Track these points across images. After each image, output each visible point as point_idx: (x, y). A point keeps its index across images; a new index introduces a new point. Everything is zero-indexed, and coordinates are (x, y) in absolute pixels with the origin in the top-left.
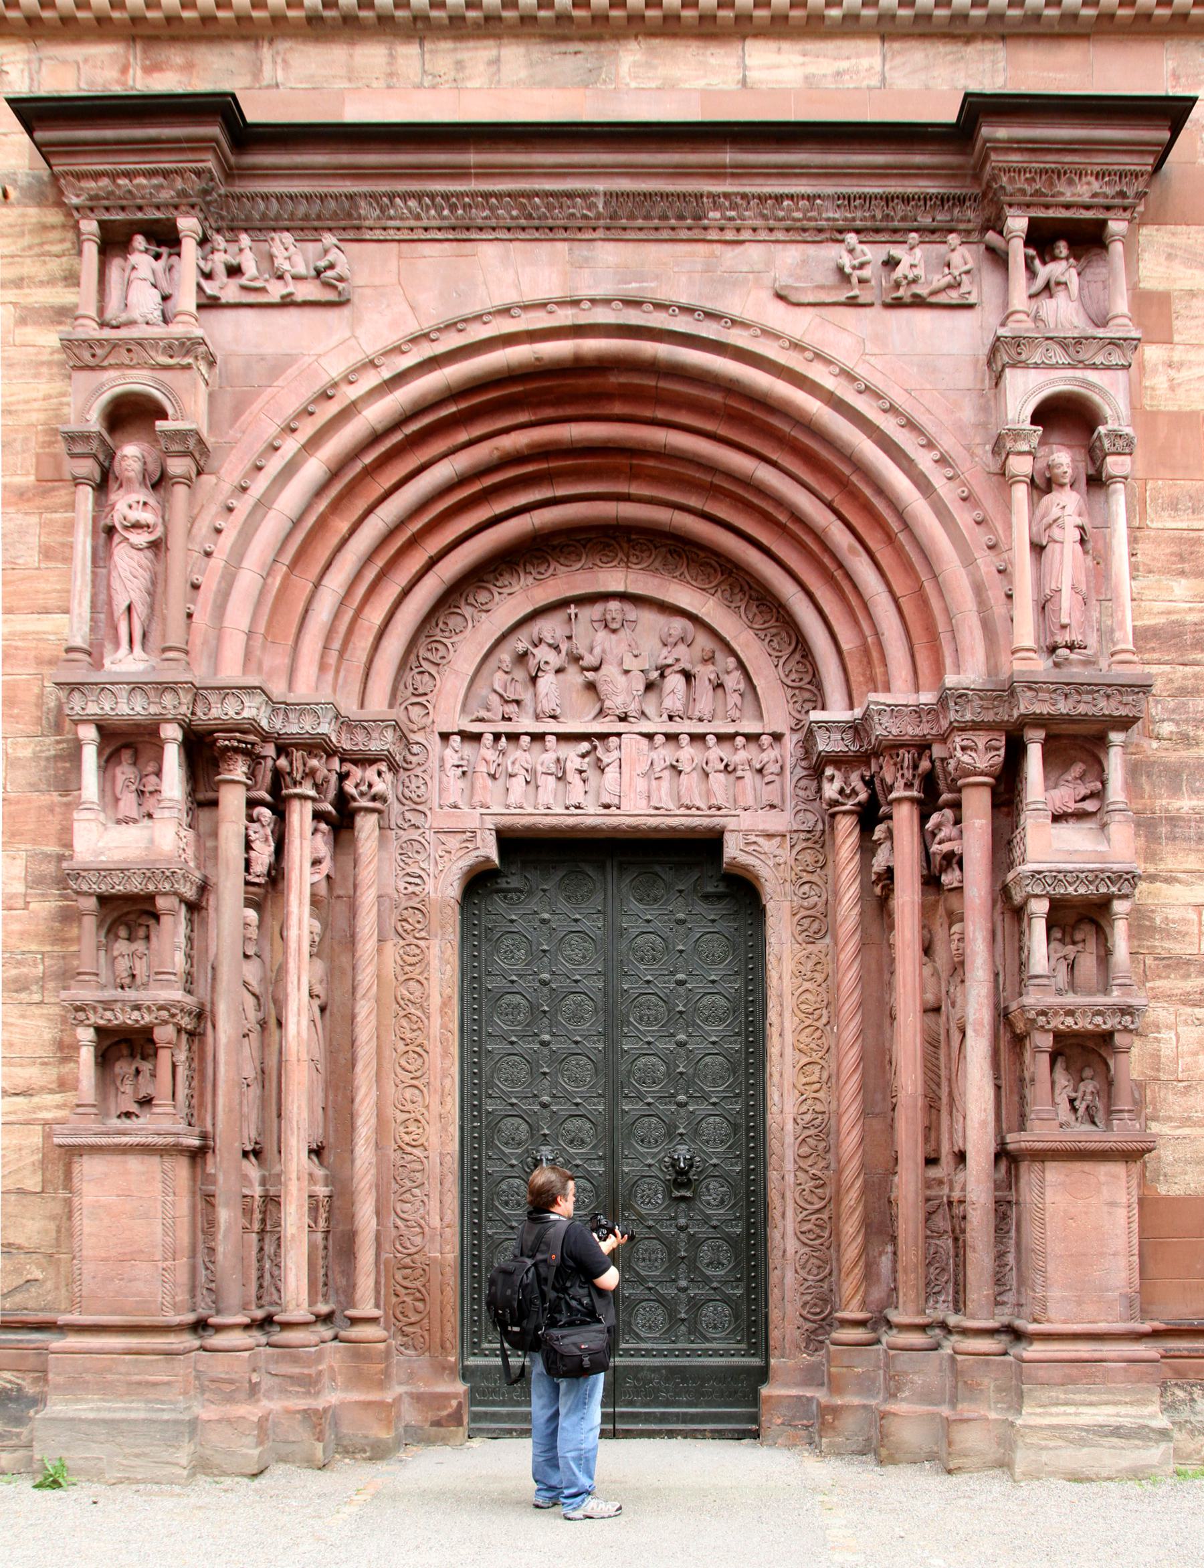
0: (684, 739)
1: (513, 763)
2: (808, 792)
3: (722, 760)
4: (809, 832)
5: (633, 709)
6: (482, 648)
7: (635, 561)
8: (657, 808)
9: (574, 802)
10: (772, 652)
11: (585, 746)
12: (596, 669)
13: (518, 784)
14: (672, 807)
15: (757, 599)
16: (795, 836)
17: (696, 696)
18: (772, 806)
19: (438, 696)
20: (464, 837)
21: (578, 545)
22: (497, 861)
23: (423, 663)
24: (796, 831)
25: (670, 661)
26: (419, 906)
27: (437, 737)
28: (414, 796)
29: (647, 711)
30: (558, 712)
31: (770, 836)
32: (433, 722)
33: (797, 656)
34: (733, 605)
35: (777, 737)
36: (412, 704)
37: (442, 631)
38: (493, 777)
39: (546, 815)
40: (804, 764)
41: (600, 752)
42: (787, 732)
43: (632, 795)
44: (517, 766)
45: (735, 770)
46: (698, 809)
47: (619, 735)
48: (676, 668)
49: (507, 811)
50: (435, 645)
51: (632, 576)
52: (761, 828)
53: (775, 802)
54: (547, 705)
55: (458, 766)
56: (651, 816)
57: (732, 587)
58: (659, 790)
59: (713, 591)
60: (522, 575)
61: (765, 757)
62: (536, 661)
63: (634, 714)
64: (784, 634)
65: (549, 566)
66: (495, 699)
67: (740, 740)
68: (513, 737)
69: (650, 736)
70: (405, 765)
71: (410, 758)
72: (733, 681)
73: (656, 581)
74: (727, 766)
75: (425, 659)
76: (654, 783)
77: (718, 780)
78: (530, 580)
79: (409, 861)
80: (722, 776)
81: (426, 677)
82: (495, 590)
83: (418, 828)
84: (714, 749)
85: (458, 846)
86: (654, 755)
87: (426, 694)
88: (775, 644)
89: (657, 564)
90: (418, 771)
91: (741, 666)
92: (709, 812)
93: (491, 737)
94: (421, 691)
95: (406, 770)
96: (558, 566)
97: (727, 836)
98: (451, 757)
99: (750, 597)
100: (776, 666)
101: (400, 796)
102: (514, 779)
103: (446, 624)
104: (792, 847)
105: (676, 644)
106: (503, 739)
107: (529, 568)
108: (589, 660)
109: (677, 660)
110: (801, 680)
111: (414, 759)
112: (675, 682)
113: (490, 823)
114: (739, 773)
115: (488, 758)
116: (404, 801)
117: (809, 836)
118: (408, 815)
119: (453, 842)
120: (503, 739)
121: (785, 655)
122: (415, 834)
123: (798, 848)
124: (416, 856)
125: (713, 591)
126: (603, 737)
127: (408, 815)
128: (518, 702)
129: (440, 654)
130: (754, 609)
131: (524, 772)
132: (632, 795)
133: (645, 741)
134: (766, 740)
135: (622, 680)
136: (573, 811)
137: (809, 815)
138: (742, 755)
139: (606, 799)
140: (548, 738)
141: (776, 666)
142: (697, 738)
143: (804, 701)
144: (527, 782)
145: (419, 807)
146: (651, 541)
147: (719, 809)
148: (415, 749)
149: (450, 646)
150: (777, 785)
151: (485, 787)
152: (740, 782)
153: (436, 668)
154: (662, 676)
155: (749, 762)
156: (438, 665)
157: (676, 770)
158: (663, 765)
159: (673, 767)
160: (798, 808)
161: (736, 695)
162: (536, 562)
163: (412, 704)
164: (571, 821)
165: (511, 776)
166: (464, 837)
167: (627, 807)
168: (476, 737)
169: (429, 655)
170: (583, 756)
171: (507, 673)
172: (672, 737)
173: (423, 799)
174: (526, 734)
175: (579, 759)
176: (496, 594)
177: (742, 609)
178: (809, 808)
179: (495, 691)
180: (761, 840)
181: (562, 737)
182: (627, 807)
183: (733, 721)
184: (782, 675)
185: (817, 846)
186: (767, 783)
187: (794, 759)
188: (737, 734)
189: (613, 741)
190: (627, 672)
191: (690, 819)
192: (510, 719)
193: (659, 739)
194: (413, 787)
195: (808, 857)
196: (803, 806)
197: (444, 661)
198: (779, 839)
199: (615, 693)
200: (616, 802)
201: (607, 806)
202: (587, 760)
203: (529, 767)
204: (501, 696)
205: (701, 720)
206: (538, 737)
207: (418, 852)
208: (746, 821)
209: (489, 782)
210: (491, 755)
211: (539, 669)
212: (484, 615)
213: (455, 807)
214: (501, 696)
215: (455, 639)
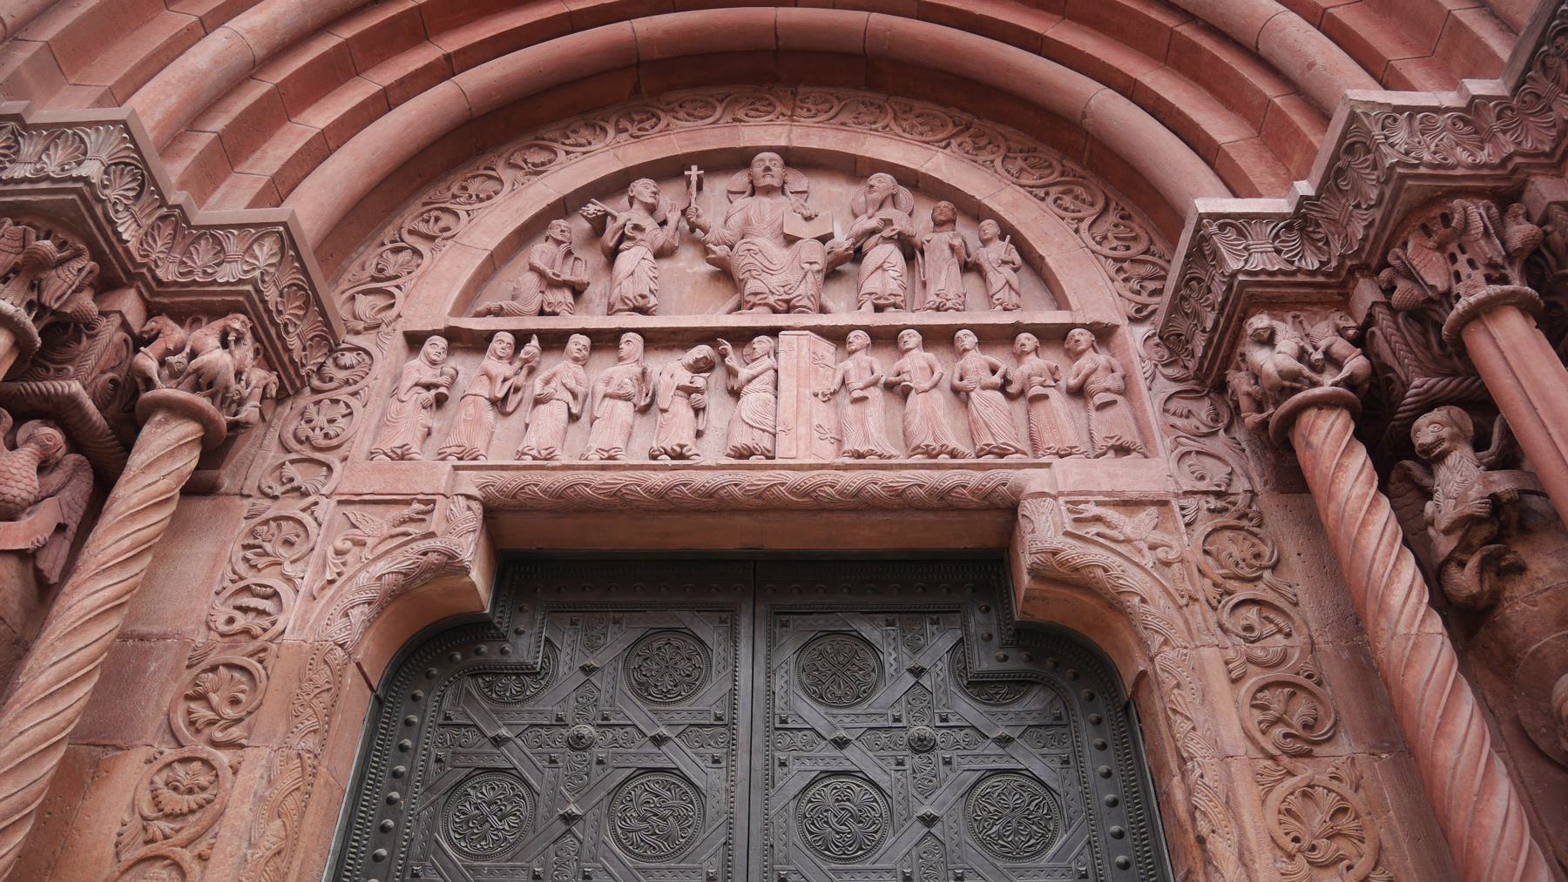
0: (912, 339)
1: (547, 382)
2: (1193, 422)
3: (994, 371)
4: (1219, 495)
5: (805, 290)
8: (860, 456)
9: (671, 443)
10: (1064, 213)
11: (702, 351)
14: (894, 452)
15: (1021, 151)
16: (1191, 502)
17: (929, 275)
18: (1122, 450)
19: (419, 277)
20: (406, 511)
21: (711, 100)
22: (478, 576)
23: (406, 236)
25: (873, 223)
26: (251, 663)
27: (399, 341)
29: (829, 304)
30: (652, 301)
31: (1130, 504)
32: (399, 316)
33: (1112, 218)
35: (1103, 334)
36: (367, 292)
37: (454, 197)
38: (499, 404)
40: (1170, 371)
41: (733, 360)
42: (1123, 323)
44: (553, 384)
46: (953, 455)
47: (773, 332)
48: (887, 233)
51: (797, 131)
52: (1104, 488)
53: (1130, 436)
54: (629, 289)
55: (428, 387)
56: (846, 468)
57: (975, 137)
59: (943, 144)
60: (611, 132)
61: (1086, 362)
62: (620, 222)
63: (805, 302)
64: (1079, 190)
66: (531, 279)
67: (1027, 340)
68: (554, 341)
69: (837, 336)
71: (330, 369)
72: (996, 252)
74: (1007, 381)
75: (410, 232)
76: (851, 410)
77: (987, 404)
78: (625, 136)
79: (262, 562)
80: (998, 395)
81: (405, 256)
84: (973, 353)
85: (386, 531)
86: (849, 364)
87: (397, 277)
89: (842, 118)
90: (342, 394)
91: (1007, 231)
93: (509, 338)
94: (390, 272)
95: (315, 391)
97: (1028, 507)
98: (418, 368)
99: (1009, 150)
100: (1077, 231)
101: (289, 436)
102: (542, 407)
103: (465, 188)
105: (881, 206)
106: (535, 342)
107: (624, 123)
109: (888, 222)
110: (1128, 248)
113: (470, 483)
114: (1036, 390)
116: (293, 444)
117: (1220, 504)
118: (290, 470)
119: (377, 523)
120: (535, 342)
121: (1089, 213)
122: (293, 507)
124: (282, 551)
125: (943, 144)
126: (742, 337)
127: (290, 470)
128: (577, 290)
129: (441, 224)
130: (1020, 163)
131: (568, 397)
132: (803, 430)
133: (826, 348)
134: (1082, 337)
135: (780, 255)
136: (665, 460)
138: (1033, 363)
139: (743, 438)
141: (1077, 231)
143: (1144, 279)
144: (573, 418)
148: (348, 358)
150: (1122, 408)
151: (477, 421)
152: (1040, 409)
154: (857, 255)
155: (1053, 372)
156: (432, 238)
157: (898, 391)
158: (868, 378)
159: (889, 387)
160: (1181, 449)
161: (1007, 271)
162: (637, 118)
164: (658, 479)
165: (538, 401)
166: (406, 511)
169: (423, 228)
170: (698, 367)
171: (559, 243)
173: (335, 442)
174: (583, 332)
175: (690, 374)
176: (562, 154)
177: (998, 162)
178: (1206, 449)
179: (533, 268)
180: (1110, 514)
181: (657, 340)
182: (787, 450)
183: (1005, 309)
184: (1092, 244)
185: (1244, 523)
186: (1102, 407)
187: (1149, 366)
188: (1018, 328)
189: (762, 343)
190: (790, 240)
191: (936, 474)
192: (554, 314)
193: (858, 339)
194: (320, 420)
195: (1234, 548)
198: (1153, 510)
199: (768, 271)
200: (766, 442)
201: (743, 453)
203: (580, 390)
204: (541, 275)
207: (288, 543)
208: (1069, 474)
209: (490, 415)
210: (502, 369)
211: (623, 238)
212: (534, 178)
213: (402, 458)
214: (541, 275)
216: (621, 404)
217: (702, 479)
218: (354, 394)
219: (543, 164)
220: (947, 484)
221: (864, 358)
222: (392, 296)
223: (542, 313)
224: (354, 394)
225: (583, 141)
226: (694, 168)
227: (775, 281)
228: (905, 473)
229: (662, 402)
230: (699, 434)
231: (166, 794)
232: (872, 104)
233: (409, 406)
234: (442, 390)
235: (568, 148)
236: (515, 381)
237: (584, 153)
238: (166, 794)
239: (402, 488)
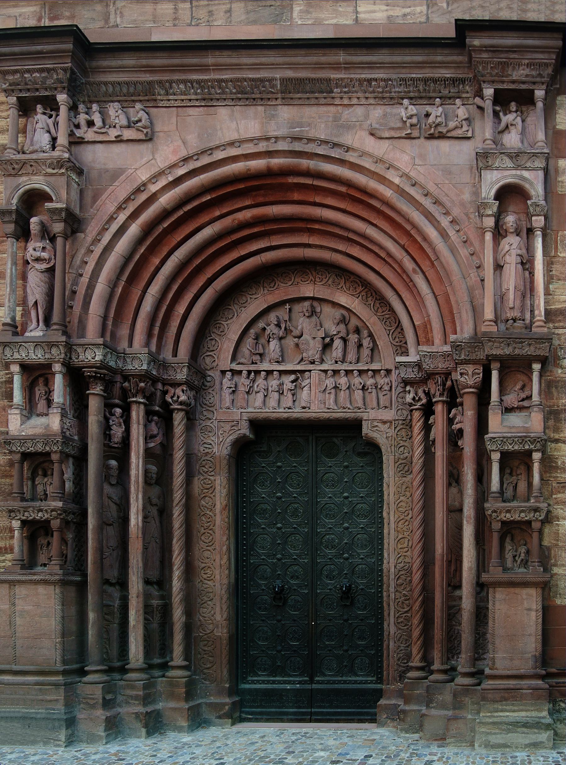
4: (404, 420)
6: (242, 326)
7: (319, 281)
8: (329, 409)
11: (293, 377)
12: (299, 337)
13: (260, 396)
16: (397, 422)
18: (386, 407)
24: (397, 420)
25: (335, 333)
28: (207, 403)
31: (384, 422)
32: (217, 365)
34: (367, 303)
35: (388, 372)
38: (248, 393)
39: (274, 412)
42: (394, 369)
43: (316, 402)
45: (368, 389)
46: (349, 409)
47: (310, 371)
48: (339, 336)
49: (255, 411)
50: (218, 325)
53: (387, 405)
55: (230, 388)
58: (329, 399)
62: (268, 333)
65: (275, 284)
69: (325, 371)
70: (203, 387)
73: (329, 291)
74: (364, 387)
79: (206, 436)
82: (249, 296)
83: (210, 419)
87: (214, 351)
88: (388, 323)
92: (354, 411)
93: (246, 372)
94: (211, 349)
96: (280, 284)
97: (363, 422)
100: (389, 335)
102: (258, 394)
104: (395, 428)
106: (253, 374)
107: (266, 285)
108: (296, 332)
111: (208, 384)
112: (338, 343)
115: (245, 383)
117: (404, 422)
119: (227, 427)
120: (253, 374)
123: (398, 429)
126: (302, 372)
133: (323, 374)
135: (312, 342)
137: (404, 412)
139: (304, 405)
140: (275, 373)
141: (389, 335)
142: (348, 373)
145: (210, 409)
146: (326, 270)
147: (360, 409)
149: (226, 326)
153: (219, 337)
158: (332, 386)
160: (399, 408)
163: (207, 356)
164: (285, 415)
167: (314, 408)
168: (240, 372)
170: (293, 382)
172: (336, 372)
173: (212, 405)
174: (264, 371)
176: (249, 299)
177: (372, 305)
180: (379, 424)
181: (281, 372)
182: (314, 408)
188: (368, 370)
192: (256, 363)
194: (208, 398)
196: (401, 407)
197: (223, 334)
200: (308, 405)
201: (304, 408)
202: (295, 384)
204: (251, 351)
205: (351, 363)
206: (269, 373)
208: (372, 414)
211: (270, 337)
213: (229, 409)
215: (229, 322)
216: (276, 393)
217: (295, 415)
218: (213, 390)
219: (244, 303)
220: (347, 417)
221: (332, 380)
222: (214, 358)
223: (253, 363)
224: (213, 390)
225: (254, 293)
226: (287, 304)
227: (310, 353)
228: (338, 414)
229: (285, 393)
230: (294, 401)
231: (204, 485)
232: (339, 275)
233: (227, 395)
234: (234, 389)
235: (251, 297)
236: (251, 385)
237: (255, 299)
238: (204, 485)
239: (231, 418)
